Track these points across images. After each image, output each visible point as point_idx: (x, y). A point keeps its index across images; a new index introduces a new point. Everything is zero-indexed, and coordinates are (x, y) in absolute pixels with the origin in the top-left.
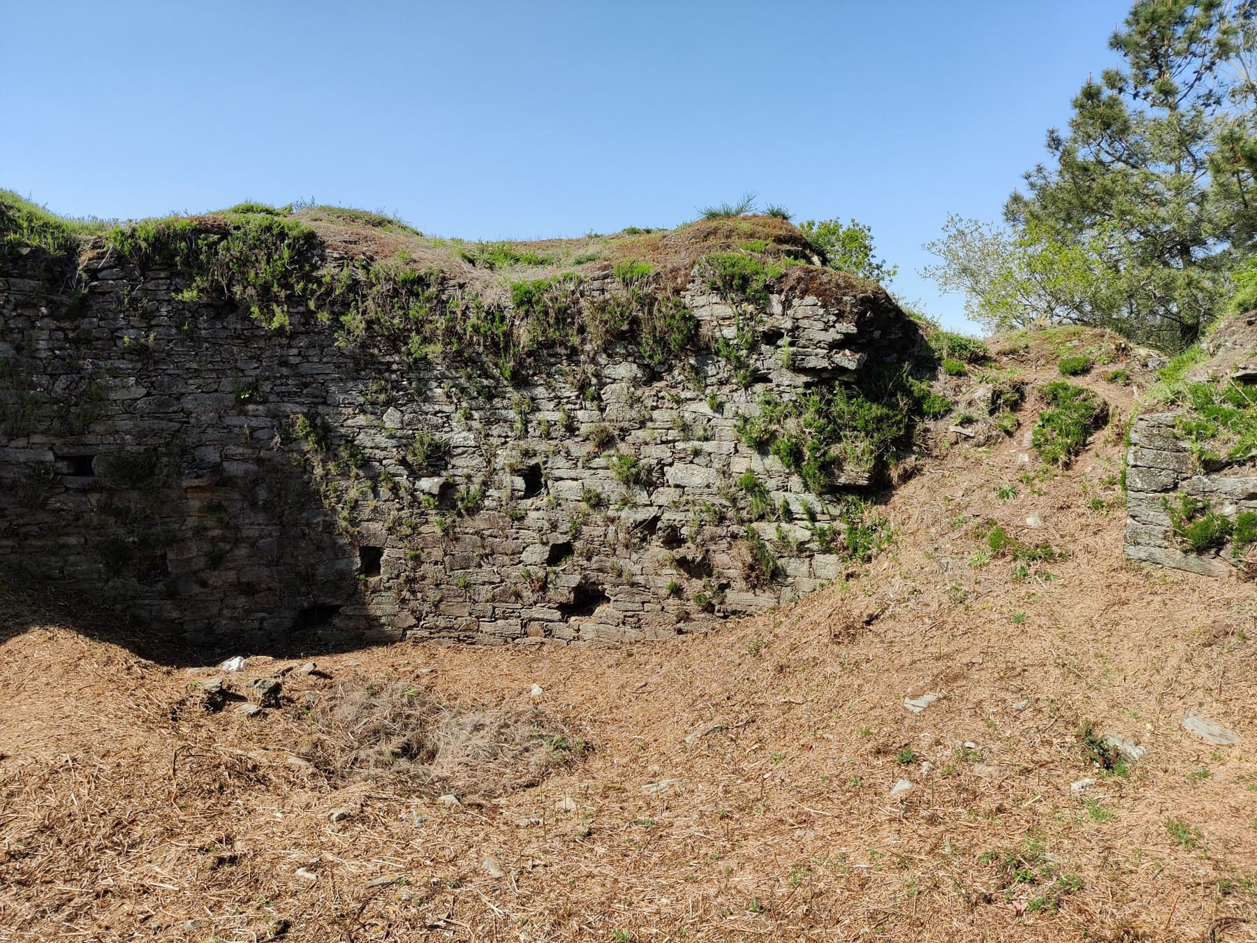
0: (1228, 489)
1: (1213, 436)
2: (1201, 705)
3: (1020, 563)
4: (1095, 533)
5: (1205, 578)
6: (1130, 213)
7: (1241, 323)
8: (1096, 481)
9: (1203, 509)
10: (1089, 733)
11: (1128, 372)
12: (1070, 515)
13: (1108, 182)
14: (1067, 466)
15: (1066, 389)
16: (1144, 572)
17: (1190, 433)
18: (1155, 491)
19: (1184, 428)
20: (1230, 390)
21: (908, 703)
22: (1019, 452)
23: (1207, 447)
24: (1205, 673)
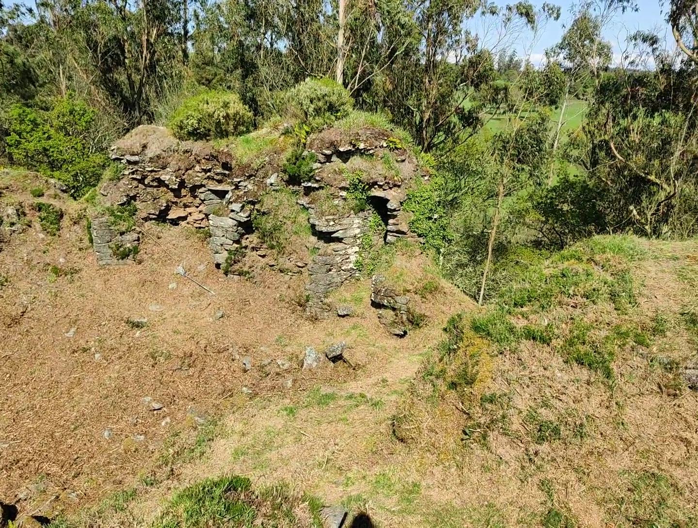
3: (69, 276)
21: (67, 335)
22: (37, 233)
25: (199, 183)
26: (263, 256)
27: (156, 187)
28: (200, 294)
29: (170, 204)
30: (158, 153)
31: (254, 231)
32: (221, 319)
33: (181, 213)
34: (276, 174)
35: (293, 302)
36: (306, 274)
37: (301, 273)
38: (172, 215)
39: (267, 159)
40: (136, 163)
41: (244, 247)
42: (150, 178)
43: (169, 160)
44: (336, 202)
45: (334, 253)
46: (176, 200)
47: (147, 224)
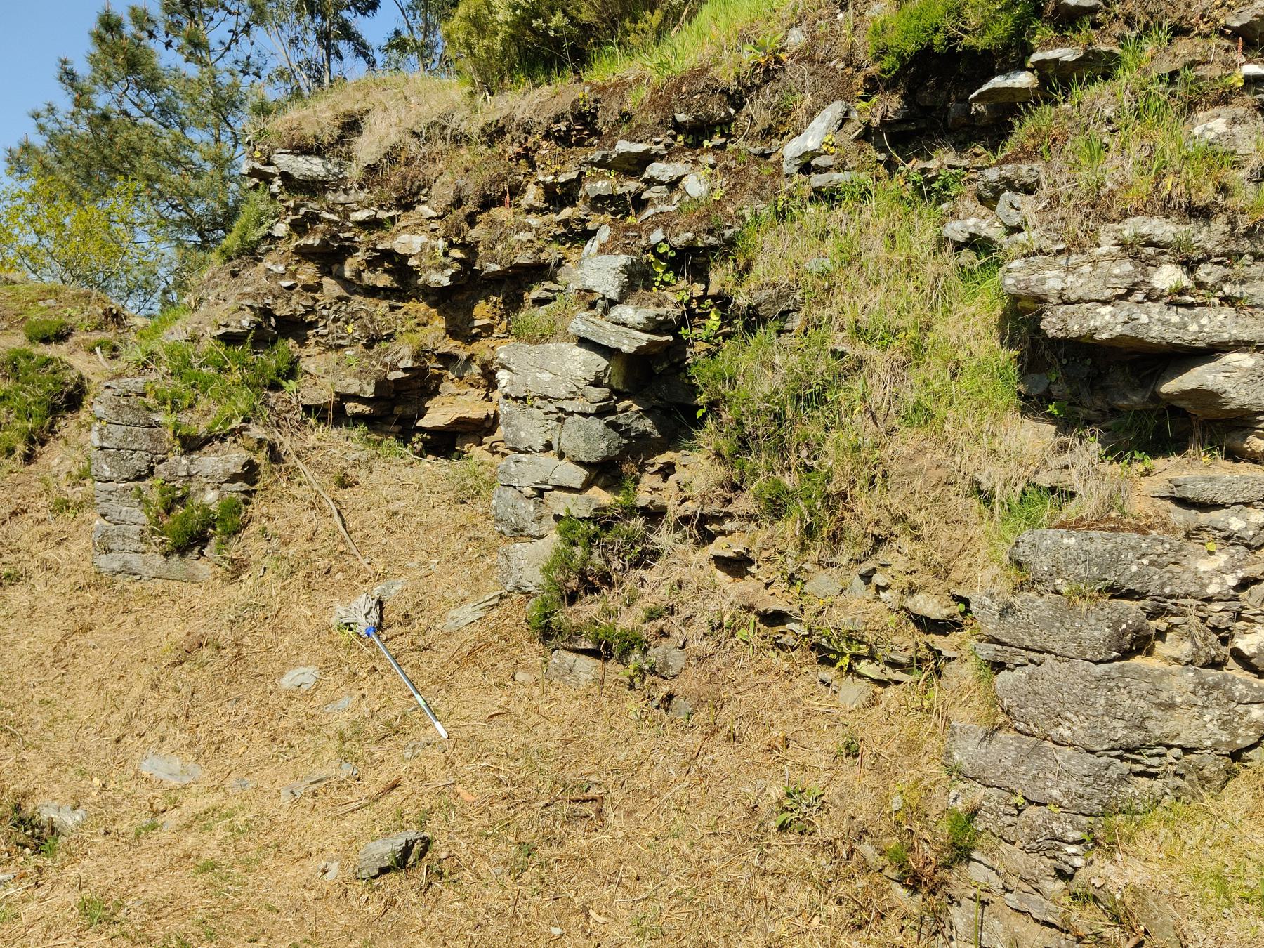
0: (208, 471)
1: (191, 406)
2: (162, 739)
4: (58, 544)
5: (187, 586)
6: (158, 180)
7: (225, 274)
8: (63, 476)
9: (183, 498)
10: (18, 808)
11: (117, 343)
12: (25, 522)
13: (133, 138)
14: (29, 458)
15: (29, 357)
16: (118, 587)
17: (164, 403)
18: (127, 480)
19: (156, 397)
20: (211, 351)
23: (185, 420)
24: (172, 697)
25: (524, 258)
26: (737, 565)
27: (386, 293)
28: (392, 731)
29: (434, 366)
30: (393, 139)
31: (700, 424)
32: (391, 880)
33: (472, 406)
34: (837, 108)
35: (866, 849)
36: (962, 673)
37: (933, 665)
38: (437, 415)
39: (797, 38)
40: (313, 187)
41: (644, 511)
42: (361, 255)
43: (431, 170)
44: (1212, 125)
45: (1180, 517)
46: (449, 346)
47: (317, 434)
